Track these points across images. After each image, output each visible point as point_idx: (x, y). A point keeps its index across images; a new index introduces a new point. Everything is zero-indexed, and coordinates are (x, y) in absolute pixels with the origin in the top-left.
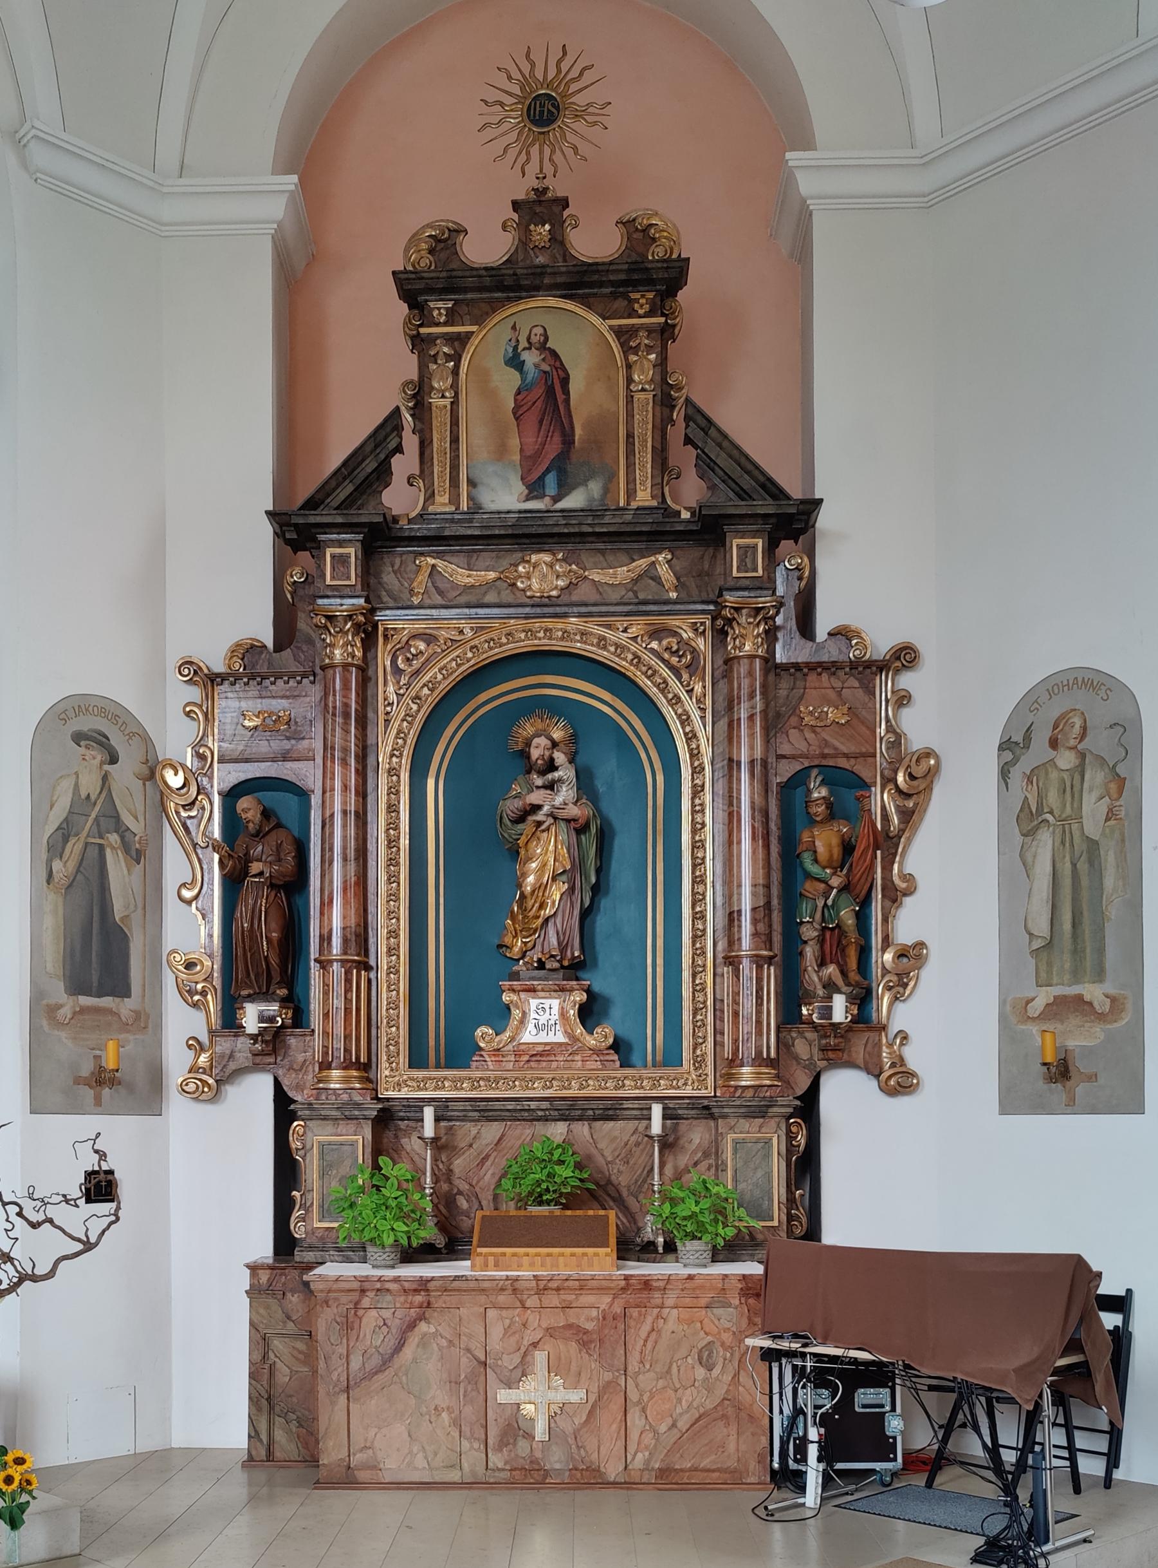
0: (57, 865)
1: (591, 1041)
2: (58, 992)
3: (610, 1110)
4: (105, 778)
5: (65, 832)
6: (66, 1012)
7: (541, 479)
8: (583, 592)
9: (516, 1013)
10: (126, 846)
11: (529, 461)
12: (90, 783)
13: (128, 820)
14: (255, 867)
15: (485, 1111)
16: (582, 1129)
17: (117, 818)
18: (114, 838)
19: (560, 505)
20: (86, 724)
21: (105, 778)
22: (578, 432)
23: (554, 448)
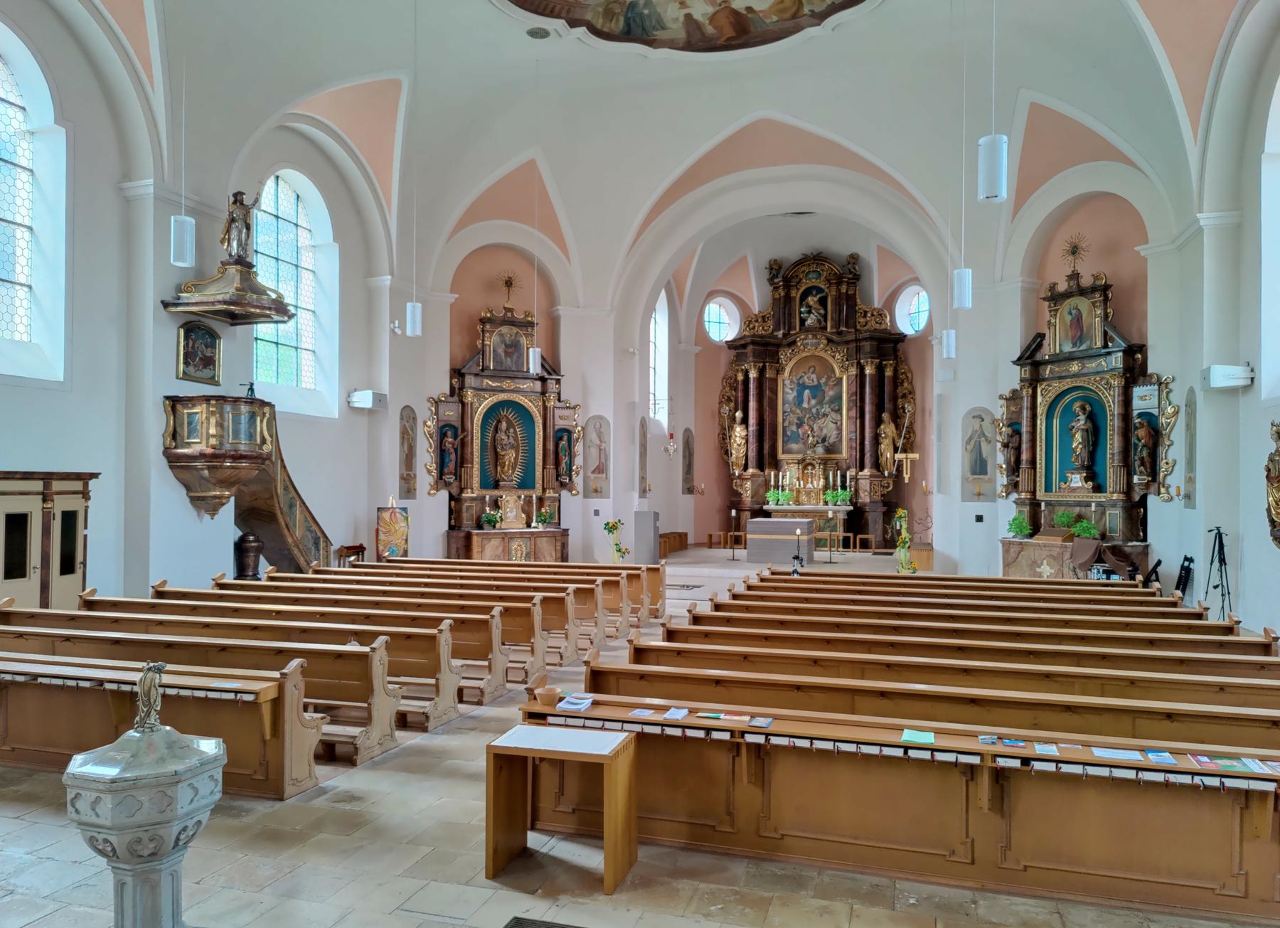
0: (968, 447)
1: (1086, 486)
2: (969, 475)
3: (1088, 505)
4: (981, 425)
5: (970, 439)
6: (970, 479)
7: (1076, 343)
8: (1085, 371)
9: (1069, 479)
10: (987, 440)
11: (1073, 338)
12: (977, 427)
13: (986, 434)
14: (1010, 445)
15: (1060, 504)
16: (1083, 509)
17: (984, 434)
18: (983, 439)
19: (1081, 348)
20: (975, 414)
21: (981, 425)
22: (1084, 329)
23: (1079, 334)
